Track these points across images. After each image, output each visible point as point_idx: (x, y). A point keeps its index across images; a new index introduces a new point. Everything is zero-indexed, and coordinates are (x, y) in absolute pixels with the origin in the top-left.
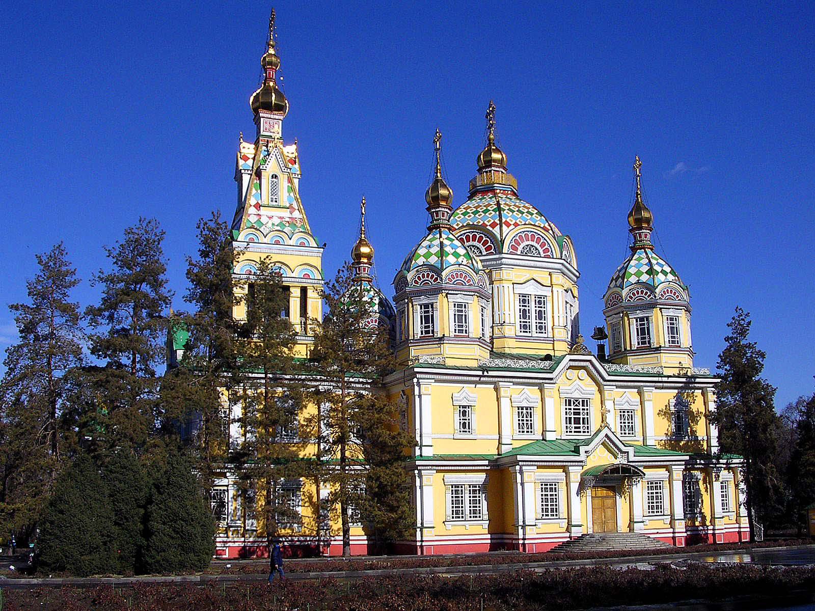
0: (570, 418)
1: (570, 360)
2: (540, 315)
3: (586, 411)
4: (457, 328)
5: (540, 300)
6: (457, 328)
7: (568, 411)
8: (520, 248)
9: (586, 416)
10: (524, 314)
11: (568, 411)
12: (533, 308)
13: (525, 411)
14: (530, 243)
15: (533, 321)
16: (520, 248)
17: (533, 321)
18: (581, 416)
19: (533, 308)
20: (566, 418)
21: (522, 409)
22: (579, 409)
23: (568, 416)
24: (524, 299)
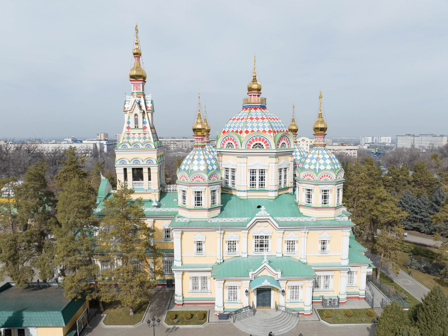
0: (258, 245)
2: (262, 179)
3: (267, 242)
4: (196, 204)
5: (262, 171)
6: (196, 204)
10: (253, 179)
11: (256, 242)
12: (257, 175)
13: (232, 242)
15: (257, 182)
16: (252, 145)
17: (257, 182)
19: (257, 175)
20: (256, 245)
23: (256, 244)
24: (253, 172)
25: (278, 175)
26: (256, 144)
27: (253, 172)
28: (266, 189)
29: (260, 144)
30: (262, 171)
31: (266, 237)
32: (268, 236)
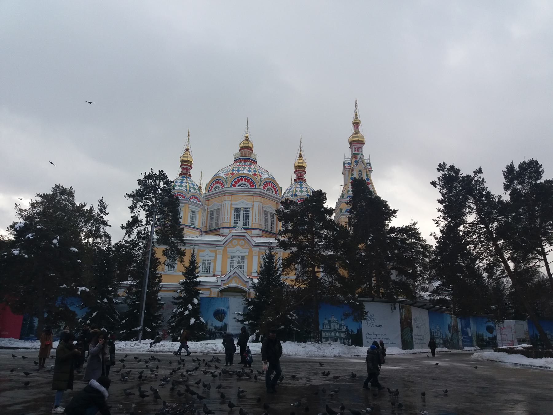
1: (233, 236)
2: (246, 217)
5: (247, 210)
7: (232, 262)
8: (237, 185)
9: (243, 265)
12: (242, 214)
13: (207, 261)
14: (243, 182)
18: (240, 265)
19: (242, 214)
20: (231, 265)
21: (205, 260)
22: (239, 261)
23: (232, 264)
24: (237, 210)
25: (263, 217)
26: (241, 184)
27: (237, 210)
28: (250, 227)
29: (245, 184)
30: (247, 210)
31: (242, 257)
32: (244, 257)
